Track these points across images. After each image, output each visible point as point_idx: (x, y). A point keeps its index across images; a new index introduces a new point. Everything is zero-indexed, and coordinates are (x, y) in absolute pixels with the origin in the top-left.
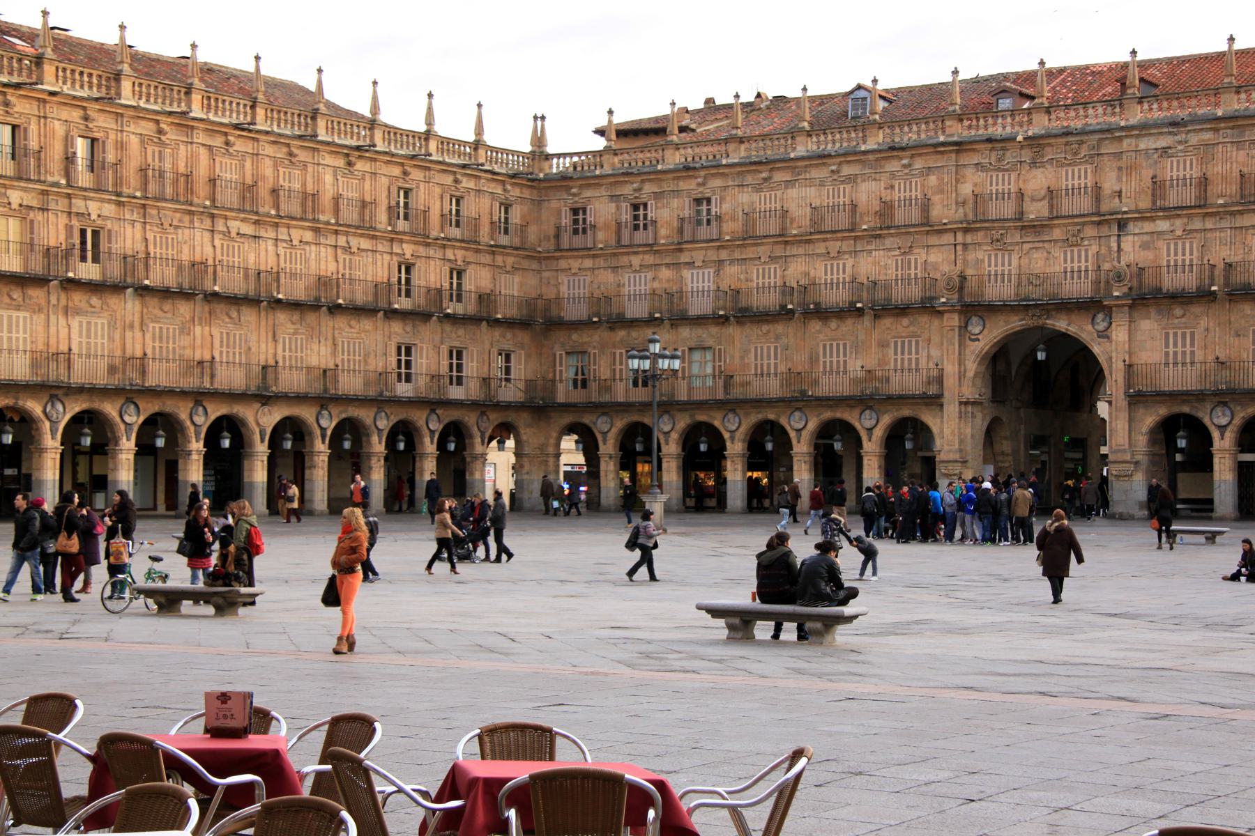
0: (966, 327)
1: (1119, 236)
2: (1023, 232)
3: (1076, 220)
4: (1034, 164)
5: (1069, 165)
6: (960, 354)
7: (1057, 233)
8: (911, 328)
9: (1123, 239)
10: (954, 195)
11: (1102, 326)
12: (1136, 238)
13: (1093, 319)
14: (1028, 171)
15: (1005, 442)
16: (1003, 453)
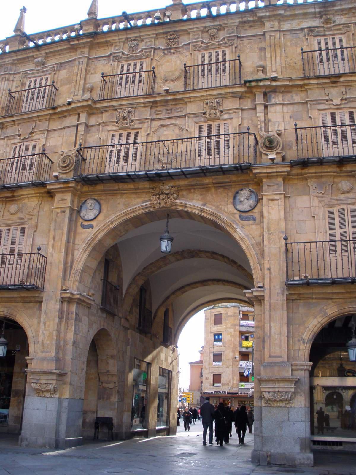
0: (79, 212)
1: (266, 107)
2: (154, 110)
3: (215, 92)
4: (168, 50)
5: (206, 48)
6: (68, 241)
7: (192, 108)
8: (19, 215)
9: (270, 109)
10: (82, 82)
11: (246, 206)
12: (285, 109)
13: (235, 197)
14: (161, 58)
15: (111, 362)
16: (108, 373)
